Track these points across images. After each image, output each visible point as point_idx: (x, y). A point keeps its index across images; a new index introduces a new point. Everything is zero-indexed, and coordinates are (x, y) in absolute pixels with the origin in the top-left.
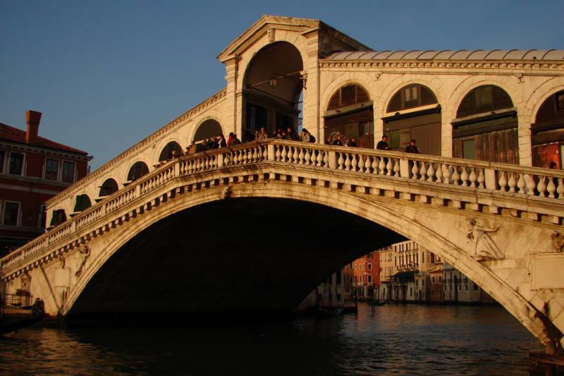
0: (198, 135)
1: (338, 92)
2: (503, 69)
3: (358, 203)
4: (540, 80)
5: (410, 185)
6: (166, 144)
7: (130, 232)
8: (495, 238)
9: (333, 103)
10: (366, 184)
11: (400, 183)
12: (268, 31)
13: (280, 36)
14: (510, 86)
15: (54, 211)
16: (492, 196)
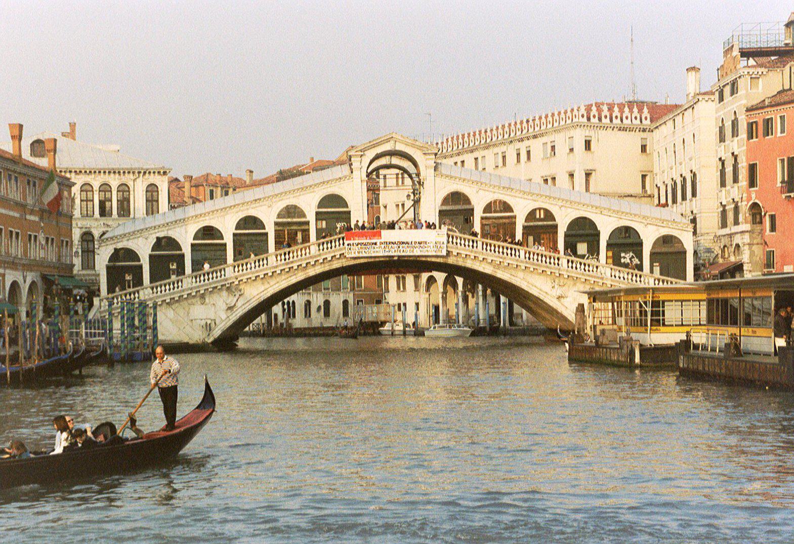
0: (322, 204)
1: (448, 195)
2: (551, 201)
3: (492, 268)
4: (569, 210)
5: (526, 262)
6: (285, 206)
7: (300, 276)
8: (564, 288)
9: (446, 201)
10: (501, 260)
11: (522, 262)
12: (392, 142)
13: (400, 147)
14: (555, 211)
15: (116, 249)
16: (567, 271)
